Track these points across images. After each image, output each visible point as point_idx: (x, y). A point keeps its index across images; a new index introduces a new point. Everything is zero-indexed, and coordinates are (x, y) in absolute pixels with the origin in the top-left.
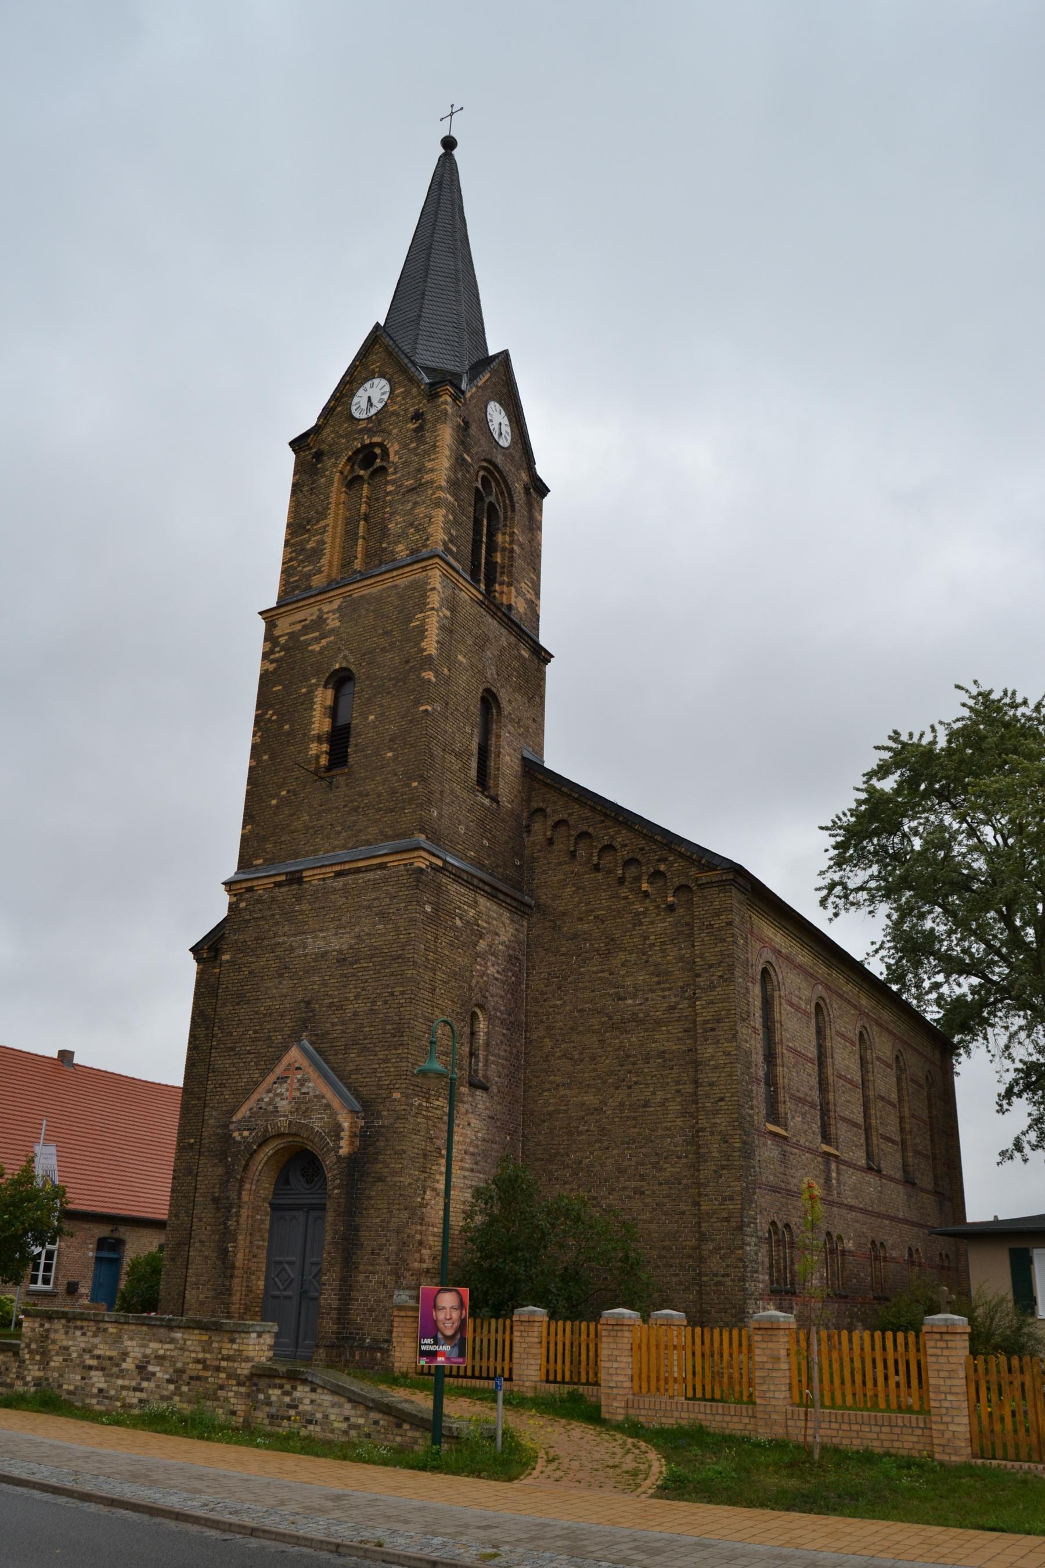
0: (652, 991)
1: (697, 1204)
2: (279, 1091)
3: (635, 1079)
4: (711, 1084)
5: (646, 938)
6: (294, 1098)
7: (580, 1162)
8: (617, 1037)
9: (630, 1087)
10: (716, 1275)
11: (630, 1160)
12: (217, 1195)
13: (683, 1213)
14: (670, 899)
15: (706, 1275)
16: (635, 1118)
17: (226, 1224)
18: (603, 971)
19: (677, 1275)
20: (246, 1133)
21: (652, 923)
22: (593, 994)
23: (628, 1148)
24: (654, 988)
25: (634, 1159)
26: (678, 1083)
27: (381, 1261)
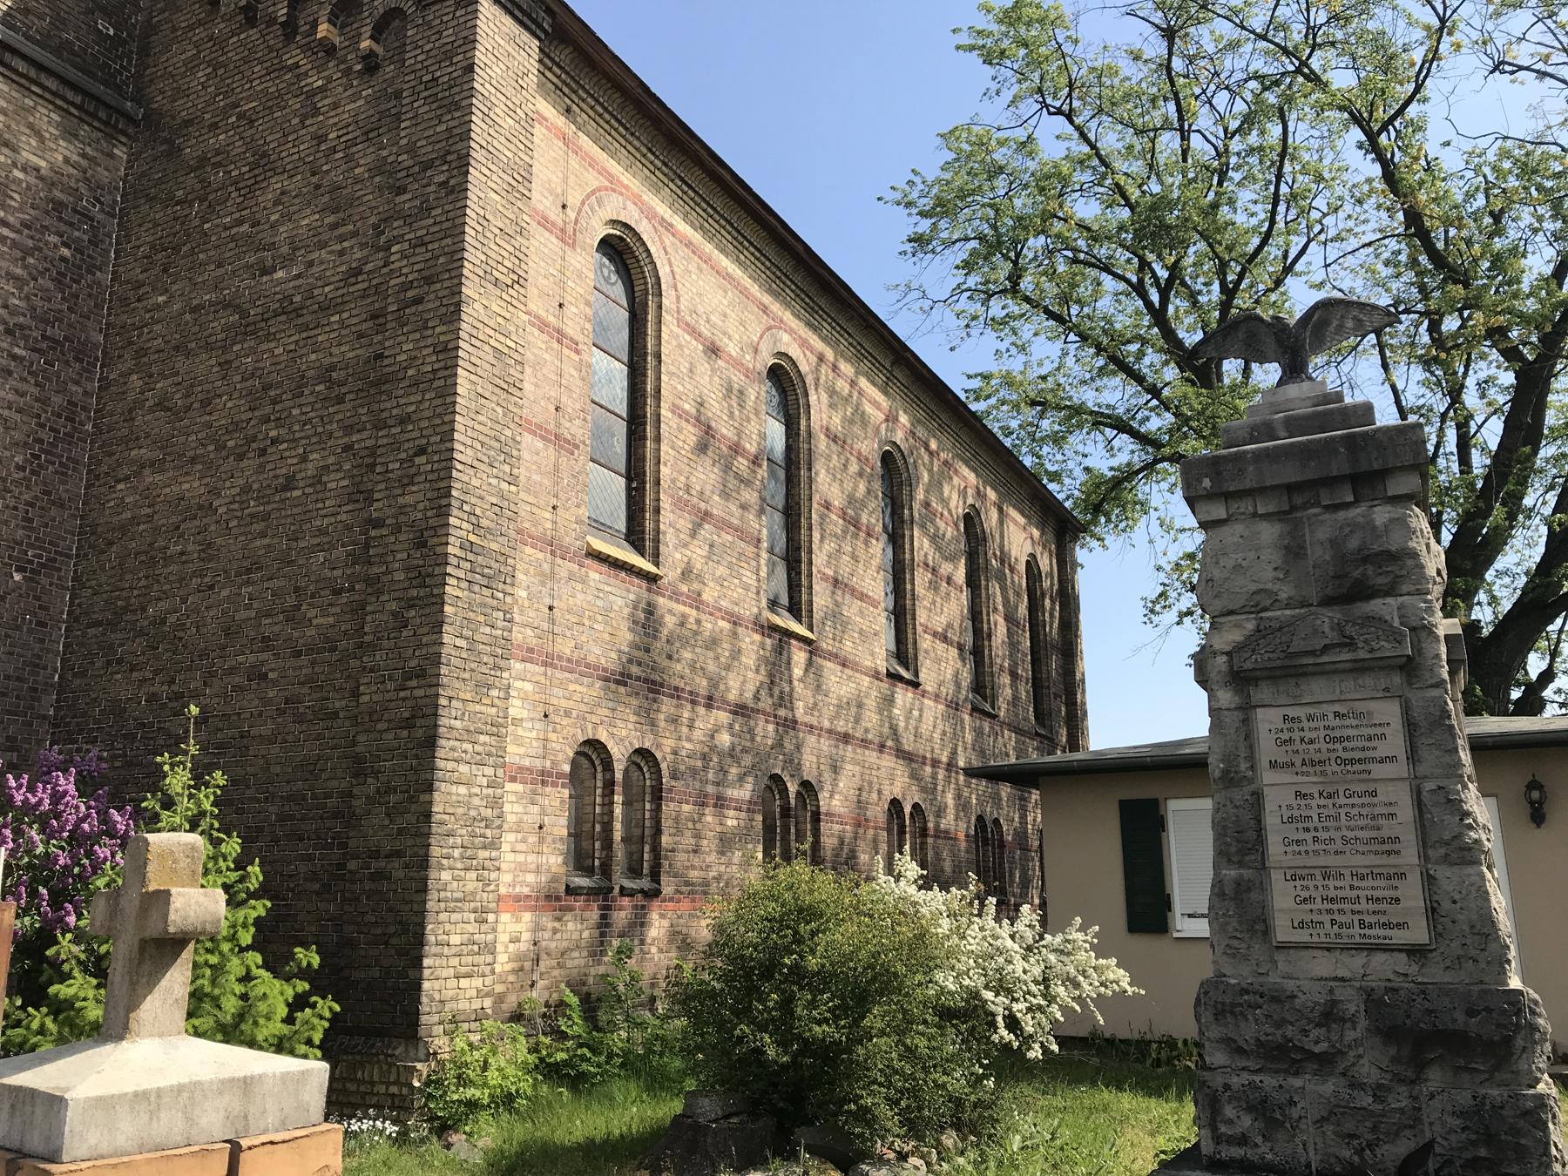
0: (323, 245)
1: (356, 694)
3: (273, 433)
4: (404, 420)
5: (321, 139)
7: (163, 622)
8: (253, 351)
9: (263, 452)
10: (375, 855)
11: (249, 607)
13: (334, 716)
14: (365, 44)
15: (356, 856)
16: (265, 517)
18: (240, 222)
19: (310, 858)
21: (335, 106)
22: (222, 271)
23: (248, 582)
24: (325, 237)
25: (256, 605)
26: (348, 429)
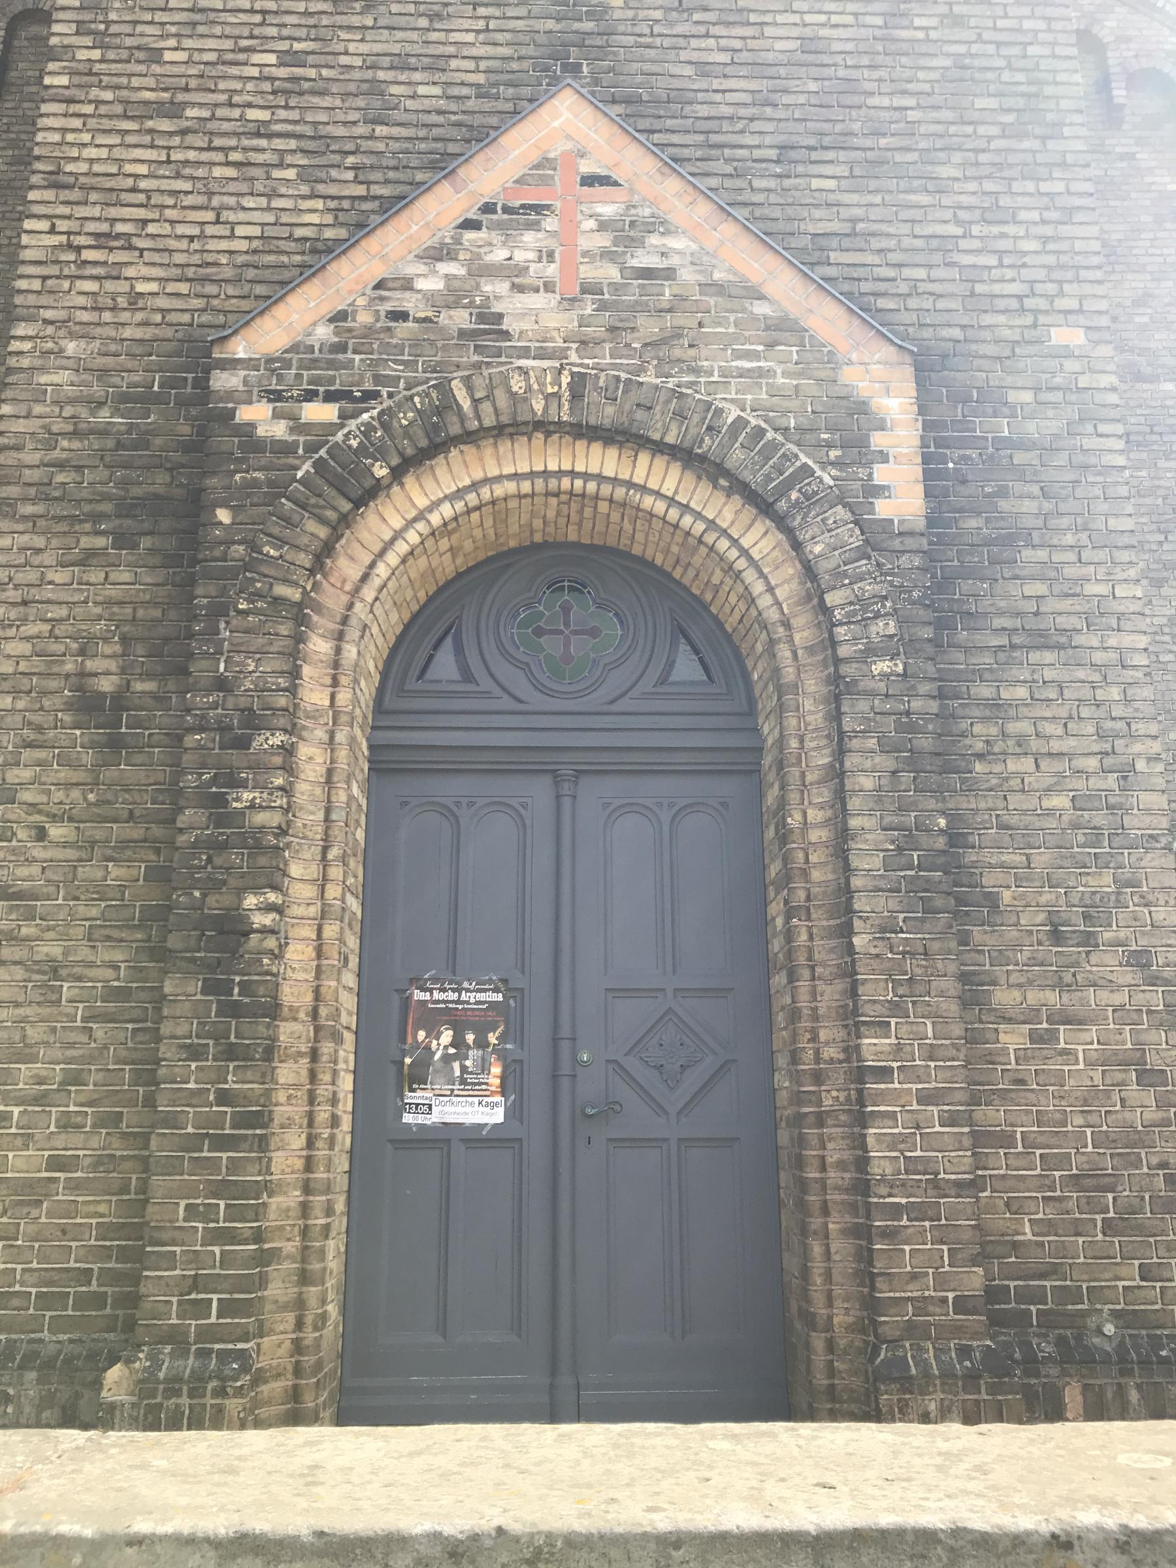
2: (499, 255)
6: (588, 288)
12: (106, 685)
17: (220, 801)
20: (320, 412)
27: (1106, 963)
